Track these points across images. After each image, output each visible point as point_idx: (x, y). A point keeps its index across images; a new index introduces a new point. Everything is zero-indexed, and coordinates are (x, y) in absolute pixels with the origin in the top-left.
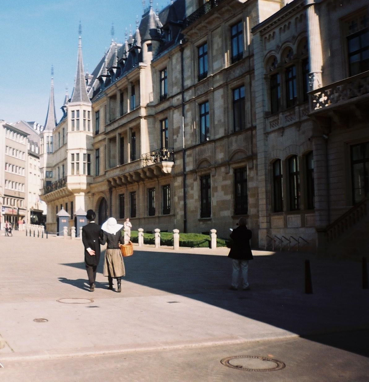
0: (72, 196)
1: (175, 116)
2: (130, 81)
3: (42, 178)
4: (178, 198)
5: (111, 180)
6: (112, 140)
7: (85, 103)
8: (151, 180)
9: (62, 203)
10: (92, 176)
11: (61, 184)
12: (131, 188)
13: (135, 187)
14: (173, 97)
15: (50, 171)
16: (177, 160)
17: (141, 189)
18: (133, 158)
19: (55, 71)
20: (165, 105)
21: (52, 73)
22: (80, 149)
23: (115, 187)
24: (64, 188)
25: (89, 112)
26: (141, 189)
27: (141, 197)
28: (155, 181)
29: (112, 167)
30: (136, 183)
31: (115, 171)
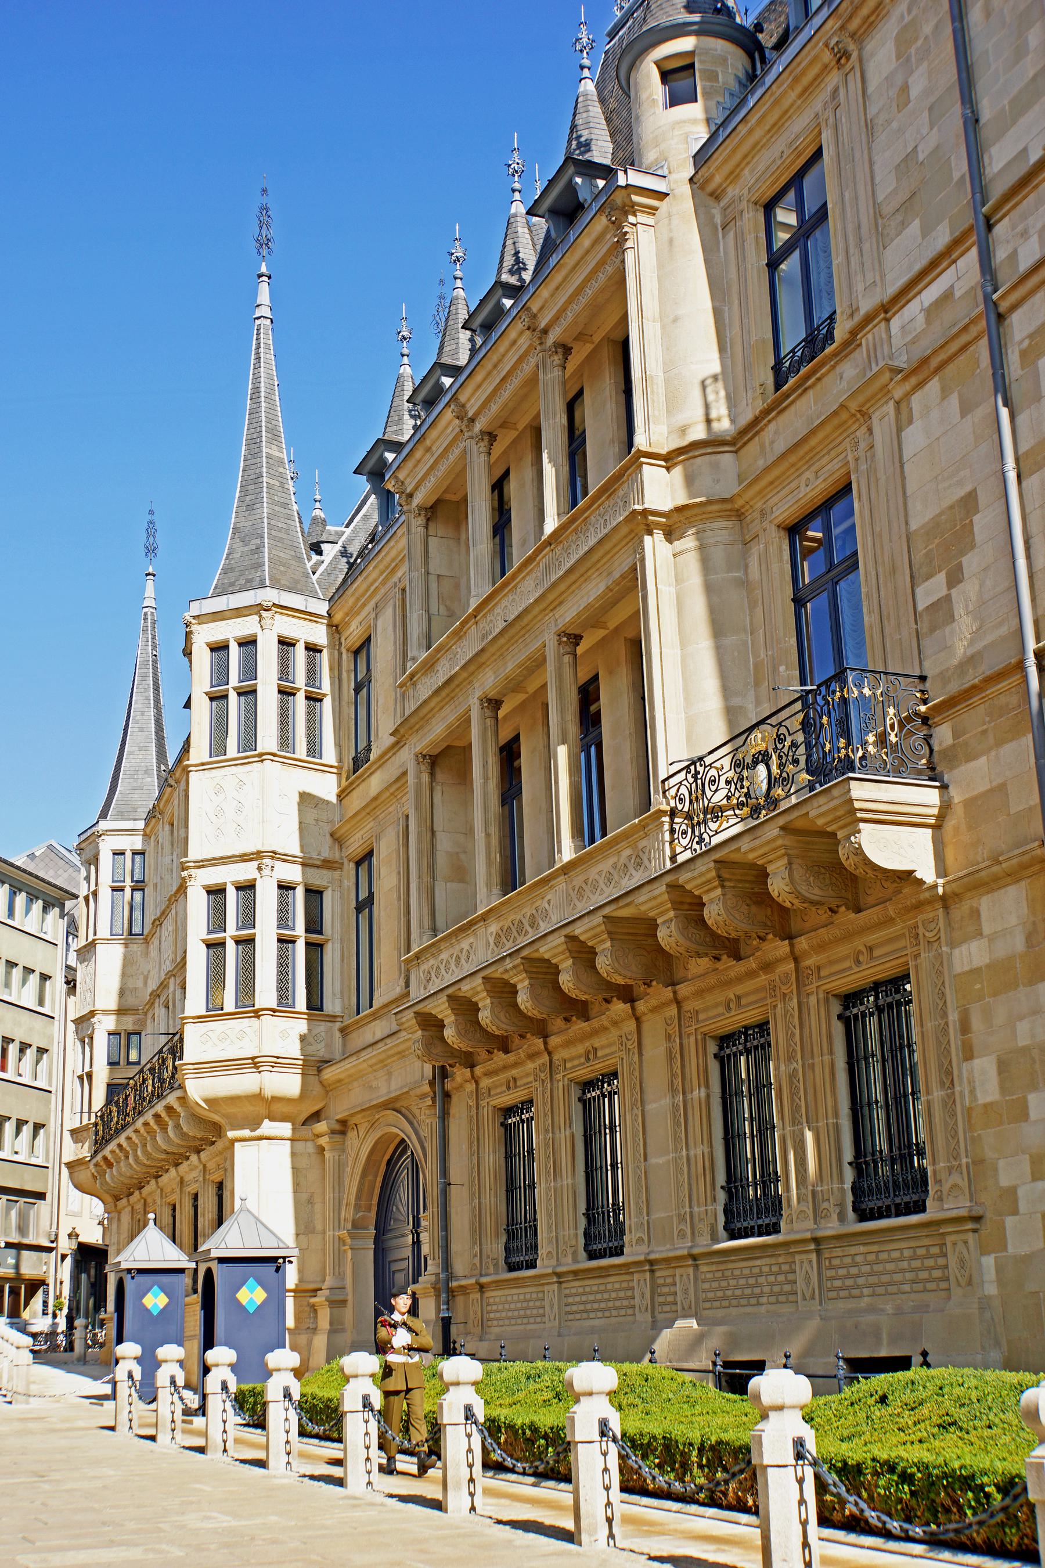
0: (220, 1145)
1: (914, 438)
2: (551, 339)
3: (87, 1069)
4: (1003, 1067)
5: (441, 1008)
6: (446, 760)
7: (295, 601)
8: (738, 968)
9: (175, 1198)
10: (332, 1019)
11: (162, 1081)
12: (574, 1052)
13: (607, 1040)
14: (887, 309)
15: (130, 1028)
16: (971, 757)
17: (655, 1049)
18: (591, 822)
19: (160, 540)
20: (840, 381)
21: (151, 550)
22: (258, 855)
23: (469, 1061)
24: (171, 1099)
25: (312, 649)
26: (655, 1049)
27: (659, 1104)
28: (767, 967)
29: (447, 930)
30: (619, 1007)
31: (465, 945)
